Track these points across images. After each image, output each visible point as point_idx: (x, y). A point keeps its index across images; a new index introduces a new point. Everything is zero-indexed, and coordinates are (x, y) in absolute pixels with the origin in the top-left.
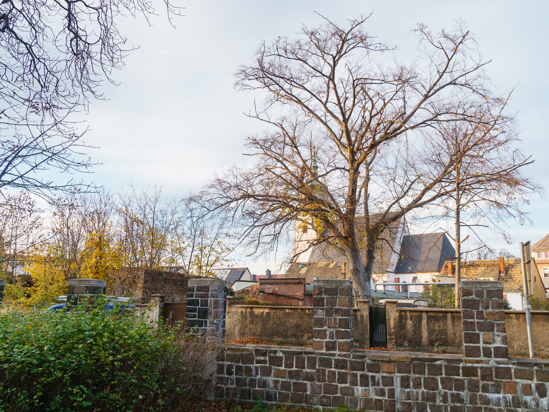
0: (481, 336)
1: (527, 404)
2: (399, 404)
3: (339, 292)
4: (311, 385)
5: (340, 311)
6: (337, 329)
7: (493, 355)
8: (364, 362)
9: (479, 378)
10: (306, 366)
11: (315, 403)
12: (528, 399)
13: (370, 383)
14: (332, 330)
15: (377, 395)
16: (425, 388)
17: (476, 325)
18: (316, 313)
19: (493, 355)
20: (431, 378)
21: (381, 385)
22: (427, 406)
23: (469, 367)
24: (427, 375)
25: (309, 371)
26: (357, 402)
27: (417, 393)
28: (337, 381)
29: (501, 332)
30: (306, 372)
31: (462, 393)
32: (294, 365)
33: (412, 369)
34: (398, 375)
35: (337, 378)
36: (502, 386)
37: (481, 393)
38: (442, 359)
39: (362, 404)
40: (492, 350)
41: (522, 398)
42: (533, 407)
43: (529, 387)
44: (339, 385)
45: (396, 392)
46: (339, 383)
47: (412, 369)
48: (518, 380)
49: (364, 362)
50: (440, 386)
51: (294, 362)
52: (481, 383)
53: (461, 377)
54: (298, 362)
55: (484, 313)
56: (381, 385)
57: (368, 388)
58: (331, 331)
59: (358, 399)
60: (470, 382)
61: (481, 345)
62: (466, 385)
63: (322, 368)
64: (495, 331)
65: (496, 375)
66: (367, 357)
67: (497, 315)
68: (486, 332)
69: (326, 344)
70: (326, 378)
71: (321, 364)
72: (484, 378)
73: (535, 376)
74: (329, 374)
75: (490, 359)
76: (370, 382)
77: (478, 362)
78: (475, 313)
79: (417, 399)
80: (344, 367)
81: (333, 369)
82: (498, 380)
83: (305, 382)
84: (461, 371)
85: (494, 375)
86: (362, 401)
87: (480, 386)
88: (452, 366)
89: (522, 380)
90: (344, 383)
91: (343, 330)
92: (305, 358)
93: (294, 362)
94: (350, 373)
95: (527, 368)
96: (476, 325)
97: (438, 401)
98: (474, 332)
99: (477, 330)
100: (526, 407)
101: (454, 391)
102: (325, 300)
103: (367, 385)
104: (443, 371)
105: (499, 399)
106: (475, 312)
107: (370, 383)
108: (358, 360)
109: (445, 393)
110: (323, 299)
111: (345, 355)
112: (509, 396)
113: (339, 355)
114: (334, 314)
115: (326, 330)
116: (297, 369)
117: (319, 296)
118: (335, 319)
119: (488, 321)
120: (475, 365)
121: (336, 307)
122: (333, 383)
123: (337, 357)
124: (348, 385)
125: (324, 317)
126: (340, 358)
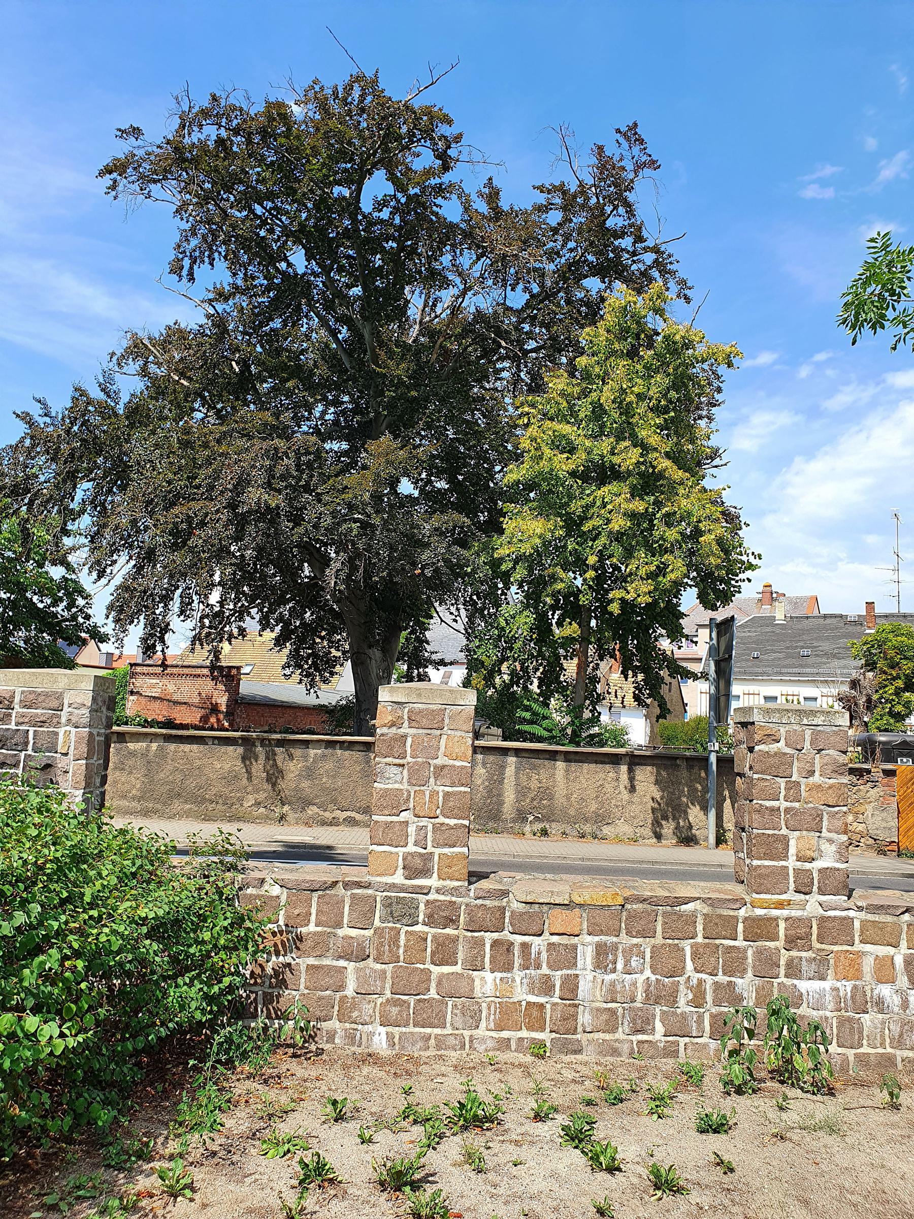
0: (792, 843)
1: (883, 1003)
2: (586, 1014)
3: (447, 721)
4: (358, 970)
5: (445, 771)
6: (437, 820)
7: (815, 889)
8: (504, 908)
9: (780, 944)
10: (345, 921)
11: (367, 1019)
12: (885, 991)
13: (517, 962)
14: (424, 822)
15: (532, 992)
16: (652, 972)
17: (782, 814)
18: (383, 777)
19: (815, 889)
20: (670, 945)
21: (544, 966)
22: (654, 1016)
23: (760, 919)
24: (659, 940)
25: (354, 933)
26: (481, 1011)
27: (634, 984)
28: (429, 959)
29: (838, 833)
30: (346, 938)
31: (739, 981)
32: (313, 918)
33: (623, 925)
34: (589, 939)
35: (429, 950)
36: (832, 962)
37: (782, 979)
38: (699, 898)
39: (492, 1017)
40: (815, 875)
41: (872, 989)
42: (896, 1009)
43: (889, 963)
44: (432, 968)
45: (581, 984)
46: (433, 963)
47: (623, 925)
48: (868, 948)
49: (504, 908)
50: (689, 965)
51: (314, 911)
52: (784, 956)
53: (740, 943)
54: (325, 908)
55: (803, 787)
56: (544, 966)
57: (509, 975)
58: (421, 824)
59: (484, 1005)
60: (759, 952)
61: (791, 863)
62: (750, 960)
63: (391, 925)
64: (824, 830)
65: (818, 935)
66: (511, 894)
67: (830, 791)
68: (804, 832)
69: (404, 859)
70: (401, 951)
71: (390, 916)
72: (791, 942)
73: (904, 936)
74: (408, 940)
75: (807, 897)
76: (516, 958)
77: (780, 905)
78: (783, 786)
79: (633, 1001)
80: (451, 920)
81: (419, 928)
82: (823, 946)
83: (342, 963)
84: (740, 927)
85: (814, 937)
86: (492, 1009)
87: (782, 962)
88: (720, 916)
89: (876, 947)
90: (447, 964)
91: (452, 822)
92: (343, 897)
93: (314, 911)
94: (465, 937)
95: (889, 919)
96: (782, 814)
97: (682, 1001)
98: (776, 832)
99: (784, 827)
100: (881, 1011)
101: (722, 978)
102: (409, 740)
103: (509, 968)
104: (700, 928)
105: (822, 994)
106: (782, 782)
107: (517, 962)
108: (487, 902)
109: (700, 982)
110: (404, 737)
111: (455, 889)
112: (846, 987)
113: (438, 891)
114: (432, 780)
115: (406, 823)
116: (319, 929)
117: (394, 730)
118: (434, 794)
119: (811, 805)
120: (775, 913)
121: (438, 762)
122: (418, 965)
123: (432, 896)
124: (458, 968)
125: (405, 786)
126: (442, 898)
